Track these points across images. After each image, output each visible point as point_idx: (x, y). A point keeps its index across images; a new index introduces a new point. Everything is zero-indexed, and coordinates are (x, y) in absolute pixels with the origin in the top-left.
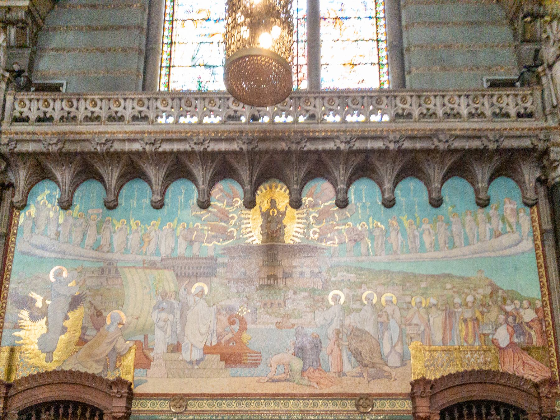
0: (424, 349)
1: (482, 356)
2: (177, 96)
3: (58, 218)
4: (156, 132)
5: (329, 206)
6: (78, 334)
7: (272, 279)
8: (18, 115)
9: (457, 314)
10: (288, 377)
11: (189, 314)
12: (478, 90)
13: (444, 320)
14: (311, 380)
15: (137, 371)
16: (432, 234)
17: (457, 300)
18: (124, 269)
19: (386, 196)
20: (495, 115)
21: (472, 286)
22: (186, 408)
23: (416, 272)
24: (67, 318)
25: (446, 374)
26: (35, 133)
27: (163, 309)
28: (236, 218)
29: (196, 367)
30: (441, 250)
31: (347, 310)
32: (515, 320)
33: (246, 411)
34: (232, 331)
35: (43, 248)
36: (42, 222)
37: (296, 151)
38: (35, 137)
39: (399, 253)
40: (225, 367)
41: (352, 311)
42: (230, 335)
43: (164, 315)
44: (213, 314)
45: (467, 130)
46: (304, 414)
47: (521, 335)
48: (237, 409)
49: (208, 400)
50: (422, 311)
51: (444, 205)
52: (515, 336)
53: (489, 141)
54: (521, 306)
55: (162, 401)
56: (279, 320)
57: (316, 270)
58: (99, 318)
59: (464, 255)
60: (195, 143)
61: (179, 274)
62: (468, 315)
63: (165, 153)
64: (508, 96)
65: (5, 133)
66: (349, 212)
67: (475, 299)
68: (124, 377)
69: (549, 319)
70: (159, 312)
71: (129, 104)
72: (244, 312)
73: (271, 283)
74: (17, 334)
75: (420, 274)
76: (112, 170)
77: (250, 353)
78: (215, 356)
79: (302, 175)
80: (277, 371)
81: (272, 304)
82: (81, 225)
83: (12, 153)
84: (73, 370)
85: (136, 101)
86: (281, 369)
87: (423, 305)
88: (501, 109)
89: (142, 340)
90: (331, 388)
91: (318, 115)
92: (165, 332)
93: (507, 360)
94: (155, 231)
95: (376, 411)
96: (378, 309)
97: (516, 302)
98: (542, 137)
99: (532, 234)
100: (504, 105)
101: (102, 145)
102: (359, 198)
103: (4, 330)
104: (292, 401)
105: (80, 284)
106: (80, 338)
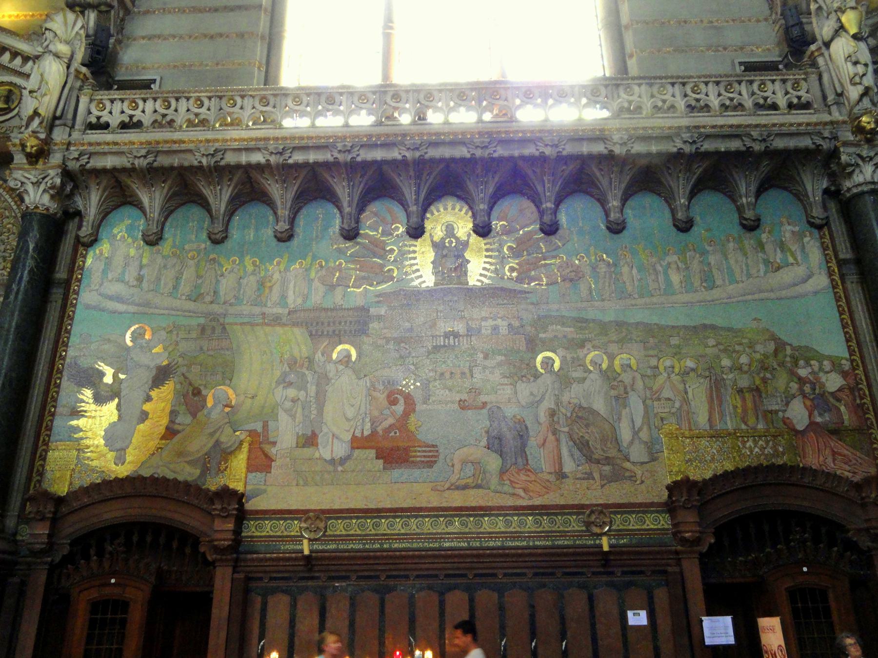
0: (683, 436)
1: (771, 443)
3: (141, 256)
5: (530, 232)
6: (165, 421)
7: (452, 337)
8: (94, 120)
11: (329, 389)
12: (731, 76)
14: (514, 485)
15: (251, 476)
17: (726, 362)
18: (235, 327)
20: (757, 106)
21: (744, 341)
22: (326, 531)
23: (663, 323)
24: (149, 399)
26: (116, 144)
28: (397, 251)
29: (340, 468)
31: (564, 379)
34: (393, 414)
35: (119, 299)
36: (118, 260)
37: (482, 159)
38: (115, 148)
39: (636, 296)
40: (384, 468)
42: (391, 421)
43: (292, 392)
45: (722, 126)
46: (506, 537)
47: (825, 412)
48: (403, 531)
50: (675, 378)
51: (695, 228)
52: (816, 412)
54: (821, 369)
56: (464, 396)
57: (516, 323)
59: (730, 298)
60: (340, 151)
61: (314, 333)
62: (744, 382)
63: (297, 166)
64: (773, 81)
65: (75, 145)
66: (559, 240)
67: (751, 360)
68: (232, 486)
69: (864, 386)
73: (449, 342)
74: (74, 423)
75: (668, 326)
76: (220, 190)
77: (419, 446)
78: (368, 451)
79: (491, 190)
80: (462, 474)
81: (452, 373)
82: (174, 265)
83: (83, 170)
84: (156, 476)
86: (469, 470)
87: (677, 370)
88: (766, 99)
89: (260, 430)
90: (546, 497)
92: (293, 417)
93: (809, 450)
94: (280, 272)
96: (609, 376)
97: (812, 362)
98: (826, 134)
99: (824, 266)
101: (210, 157)
103: (56, 417)
104: (486, 519)
105: (170, 349)
106: (167, 428)
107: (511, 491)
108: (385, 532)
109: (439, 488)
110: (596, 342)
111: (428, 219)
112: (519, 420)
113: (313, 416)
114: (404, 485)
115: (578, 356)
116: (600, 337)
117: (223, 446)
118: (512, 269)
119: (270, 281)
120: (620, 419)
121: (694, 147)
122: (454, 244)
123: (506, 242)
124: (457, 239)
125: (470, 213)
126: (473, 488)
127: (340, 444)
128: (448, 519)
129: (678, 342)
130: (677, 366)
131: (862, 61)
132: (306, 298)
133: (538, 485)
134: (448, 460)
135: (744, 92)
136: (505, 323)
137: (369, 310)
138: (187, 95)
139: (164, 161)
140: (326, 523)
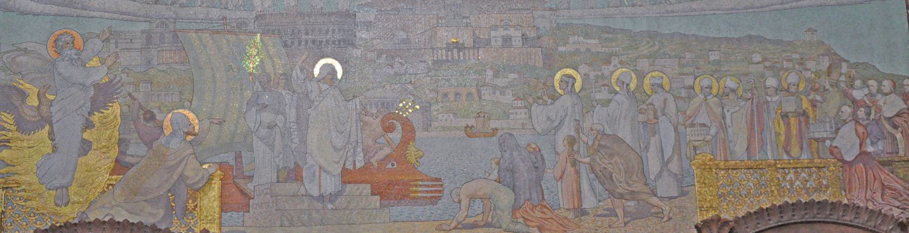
0: (718, 168)
7: (455, 51)
10: (490, 219)
14: (528, 223)
15: (226, 216)
17: (771, 82)
23: (702, 33)
27: (265, 106)
29: (330, 206)
41: (595, 103)
42: (387, 151)
43: (267, 117)
50: (712, 100)
52: (868, 141)
54: (879, 91)
56: (471, 122)
57: (532, 34)
62: (790, 107)
70: (258, 111)
77: (422, 180)
78: (362, 186)
81: (457, 94)
86: (478, 206)
87: (715, 91)
92: (272, 147)
97: (871, 82)
106: (117, 161)
109: (444, 227)
110: (624, 58)
113: (294, 146)
115: (603, 74)
116: (630, 52)
117: (189, 182)
120: (647, 148)
129: (718, 58)
130: (715, 85)
133: (555, 223)
134: (454, 196)
136: (518, 34)
137: (355, 15)
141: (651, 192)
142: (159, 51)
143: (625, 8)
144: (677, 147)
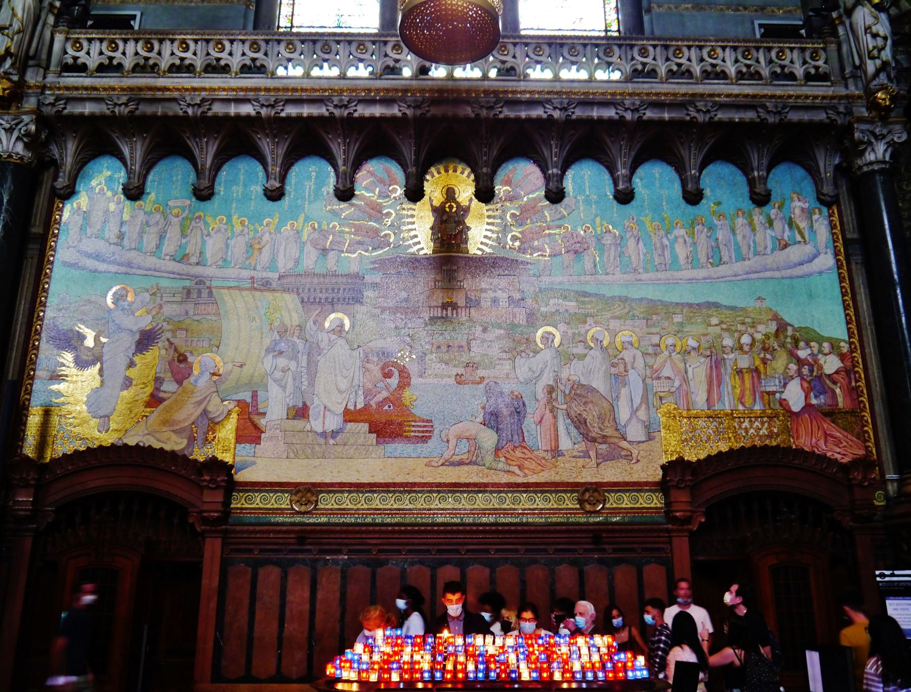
0: (681, 416)
1: (766, 424)
2: (310, 38)
3: (122, 212)
4: (277, 90)
5: (534, 199)
6: (149, 390)
7: (449, 309)
8: (70, 61)
9: (727, 361)
10: (474, 458)
11: (321, 360)
12: (749, 41)
13: (708, 371)
15: (240, 447)
16: (688, 245)
17: (728, 342)
18: (222, 291)
19: (621, 186)
20: (774, 75)
21: (748, 320)
22: (316, 505)
23: (666, 299)
24: (132, 364)
25: (714, 452)
26: (95, 89)
27: (281, 353)
28: (394, 215)
29: (332, 442)
30: (703, 267)
31: (565, 357)
32: (811, 371)
33: (410, 509)
34: (387, 387)
35: (97, 257)
36: (97, 218)
37: (487, 119)
38: (94, 94)
39: (641, 270)
41: (572, 357)
42: (385, 394)
43: (282, 362)
44: (358, 361)
45: (737, 96)
46: (500, 514)
47: (821, 394)
48: (395, 506)
49: (350, 492)
51: (704, 201)
52: (812, 395)
53: (769, 112)
54: (820, 351)
55: (279, 494)
56: (461, 371)
57: (517, 296)
58: (182, 366)
59: (735, 276)
60: (336, 106)
61: (306, 300)
62: (744, 362)
64: (792, 49)
65: (50, 89)
66: (565, 209)
67: (753, 339)
68: (220, 456)
69: (860, 369)
71: (238, 48)
72: (407, 359)
73: (447, 314)
74: (55, 387)
75: (671, 303)
76: (207, 142)
77: (415, 421)
80: (457, 450)
82: (157, 223)
84: (141, 444)
85: (247, 45)
86: (464, 446)
87: (678, 349)
88: (783, 67)
89: (249, 400)
90: (540, 474)
91: (520, 69)
92: (284, 388)
93: (802, 431)
94: (270, 233)
95: (609, 509)
97: (812, 344)
98: (842, 109)
99: (831, 244)
100: (787, 62)
101: (196, 107)
102: (580, 189)
103: (35, 381)
104: (480, 495)
105: (154, 313)
106: (152, 395)
107: (507, 468)
108: (377, 507)
109: (433, 464)
111: (427, 181)
112: (517, 396)
113: (304, 387)
114: (398, 460)
116: (603, 313)
117: (211, 416)
118: (514, 238)
119: (259, 243)
121: (708, 116)
122: (454, 210)
123: (511, 208)
124: (458, 204)
125: (472, 177)
126: (468, 464)
127: (332, 417)
128: (441, 495)
129: (680, 320)
130: (679, 344)
131: (882, 33)
132: (297, 262)
134: (443, 436)
135: (762, 60)
136: (505, 295)
138: (171, 37)
139: (147, 109)
140: (317, 496)
141: (620, 436)
142: (196, 304)
143: (599, 276)
144: (645, 398)
